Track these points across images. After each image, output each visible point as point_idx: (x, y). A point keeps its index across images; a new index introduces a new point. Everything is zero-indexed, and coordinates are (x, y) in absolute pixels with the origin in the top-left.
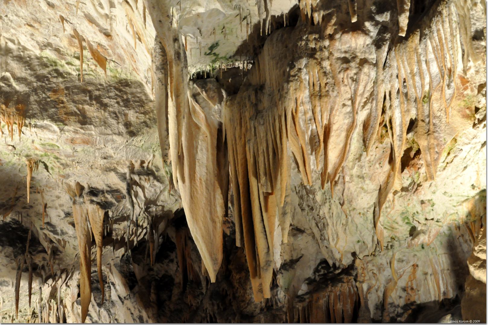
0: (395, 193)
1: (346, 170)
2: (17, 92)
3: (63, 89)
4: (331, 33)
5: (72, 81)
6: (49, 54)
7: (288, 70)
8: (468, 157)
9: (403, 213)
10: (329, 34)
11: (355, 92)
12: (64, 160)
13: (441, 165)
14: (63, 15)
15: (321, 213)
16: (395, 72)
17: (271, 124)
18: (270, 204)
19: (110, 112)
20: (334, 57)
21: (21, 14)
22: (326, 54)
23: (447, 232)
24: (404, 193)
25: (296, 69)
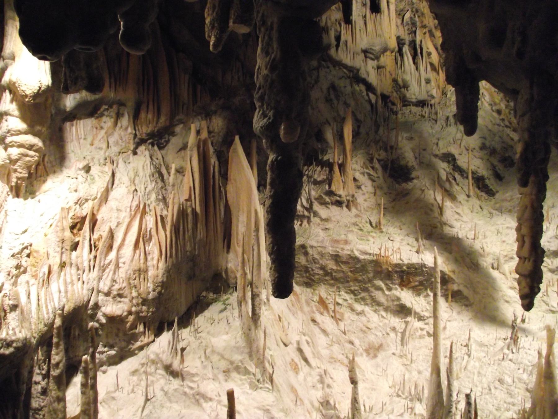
0: (96, 198)
1: (129, 216)
2: (382, 280)
3: (351, 281)
4: (130, 316)
5: (345, 287)
6: (359, 307)
7: (163, 291)
9: (93, 183)
11: (114, 273)
12: (355, 229)
13: (57, 217)
14: (344, 336)
15: (153, 185)
18: (188, 193)
19: (318, 263)
20: (128, 298)
21: (373, 336)
22: (134, 301)
23: (64, 169)
24: (89, 198)
25: (157, 291)
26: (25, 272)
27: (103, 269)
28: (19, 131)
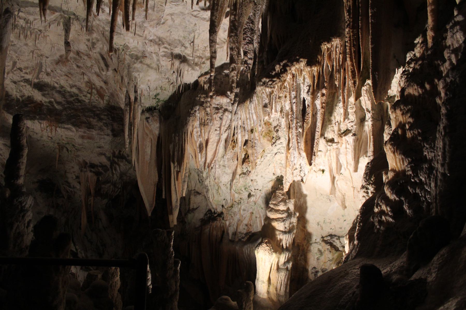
1: (217, 162)
2: (56, 109)
6: (74, 90)
9: (245, 186)
11: (221, 125)
15: (206, 183)
16: (239, 117)
21: (64, 70)
23: (265, 196)
25: (194, 111)
27: (229, 127)
28: (277, 221)
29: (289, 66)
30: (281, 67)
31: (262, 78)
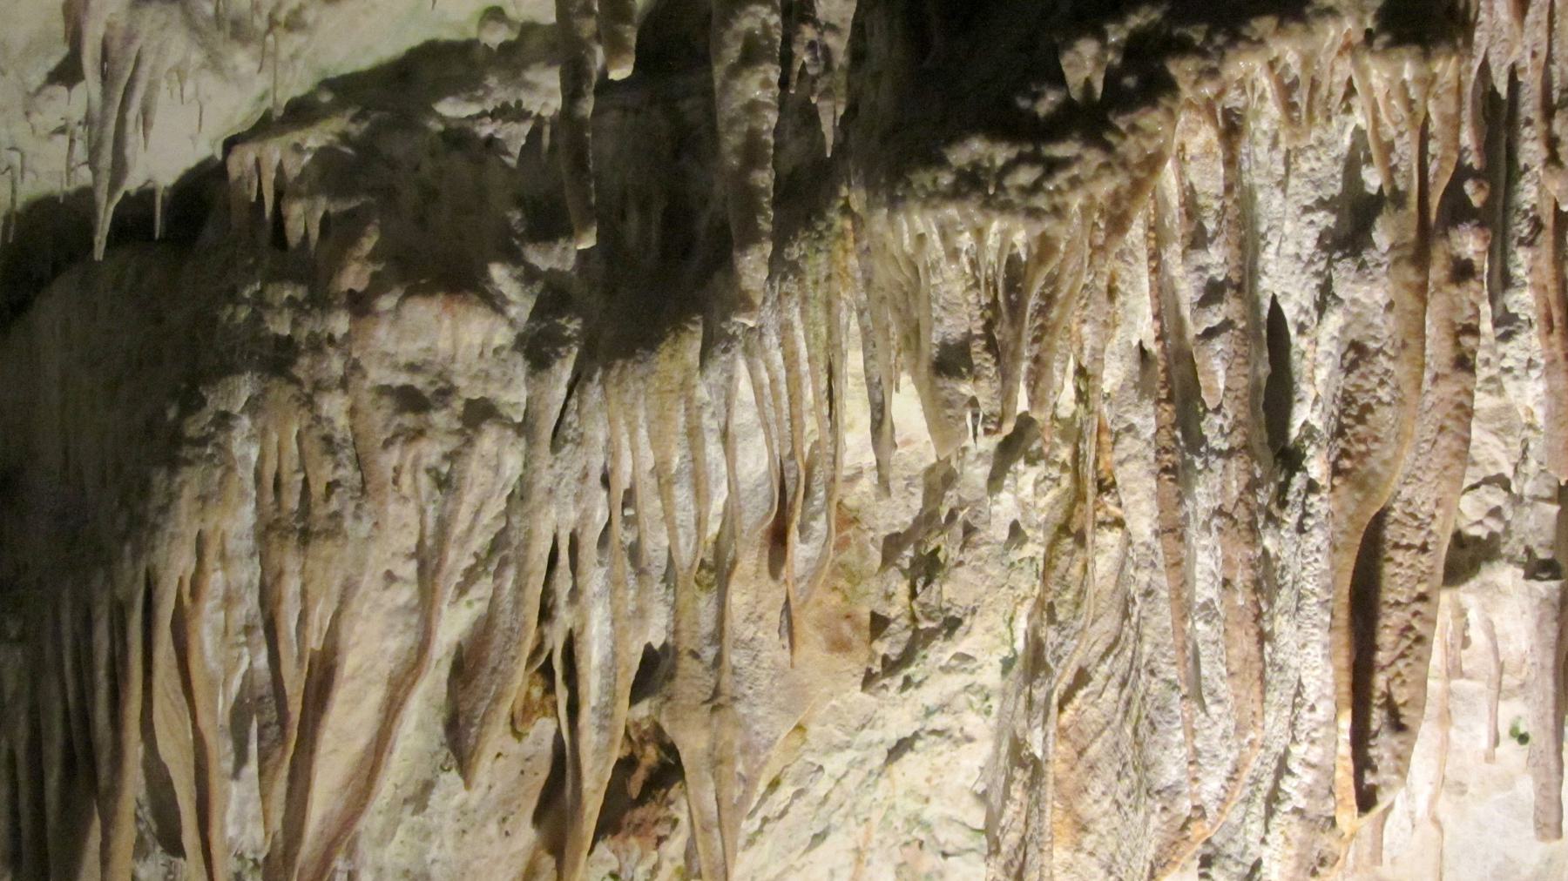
1: (364, 845)
4: (360, 288)
7: (172, 414)
8: (834, 797)
10: (351, 291)
11: (443, 525)
16: (597, 462)
17: (67, 641)
20: (368, 384)
22: (335, 365)
25: (207, 415)
26: (893, 544)
27: (501, 550)
29: (1202, 53)
30: (1113, 58)
31: (957, 137)
